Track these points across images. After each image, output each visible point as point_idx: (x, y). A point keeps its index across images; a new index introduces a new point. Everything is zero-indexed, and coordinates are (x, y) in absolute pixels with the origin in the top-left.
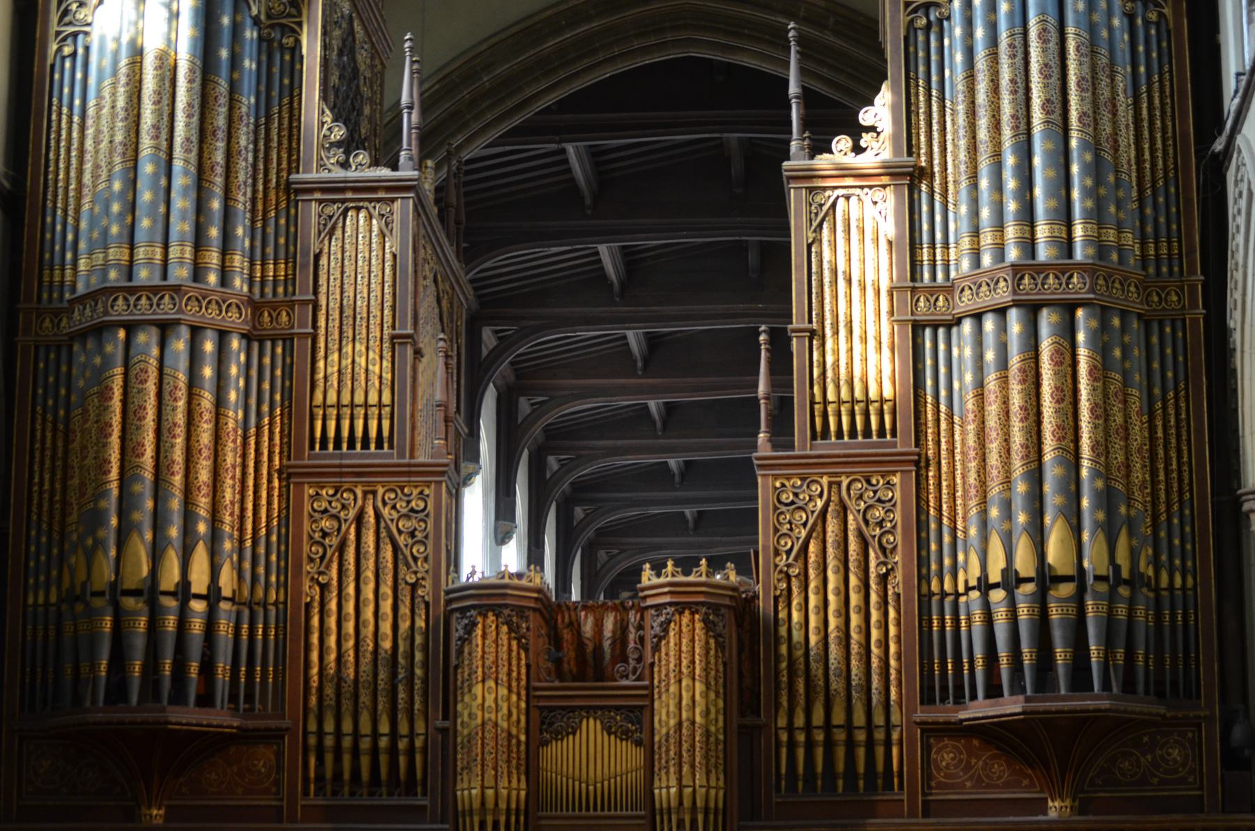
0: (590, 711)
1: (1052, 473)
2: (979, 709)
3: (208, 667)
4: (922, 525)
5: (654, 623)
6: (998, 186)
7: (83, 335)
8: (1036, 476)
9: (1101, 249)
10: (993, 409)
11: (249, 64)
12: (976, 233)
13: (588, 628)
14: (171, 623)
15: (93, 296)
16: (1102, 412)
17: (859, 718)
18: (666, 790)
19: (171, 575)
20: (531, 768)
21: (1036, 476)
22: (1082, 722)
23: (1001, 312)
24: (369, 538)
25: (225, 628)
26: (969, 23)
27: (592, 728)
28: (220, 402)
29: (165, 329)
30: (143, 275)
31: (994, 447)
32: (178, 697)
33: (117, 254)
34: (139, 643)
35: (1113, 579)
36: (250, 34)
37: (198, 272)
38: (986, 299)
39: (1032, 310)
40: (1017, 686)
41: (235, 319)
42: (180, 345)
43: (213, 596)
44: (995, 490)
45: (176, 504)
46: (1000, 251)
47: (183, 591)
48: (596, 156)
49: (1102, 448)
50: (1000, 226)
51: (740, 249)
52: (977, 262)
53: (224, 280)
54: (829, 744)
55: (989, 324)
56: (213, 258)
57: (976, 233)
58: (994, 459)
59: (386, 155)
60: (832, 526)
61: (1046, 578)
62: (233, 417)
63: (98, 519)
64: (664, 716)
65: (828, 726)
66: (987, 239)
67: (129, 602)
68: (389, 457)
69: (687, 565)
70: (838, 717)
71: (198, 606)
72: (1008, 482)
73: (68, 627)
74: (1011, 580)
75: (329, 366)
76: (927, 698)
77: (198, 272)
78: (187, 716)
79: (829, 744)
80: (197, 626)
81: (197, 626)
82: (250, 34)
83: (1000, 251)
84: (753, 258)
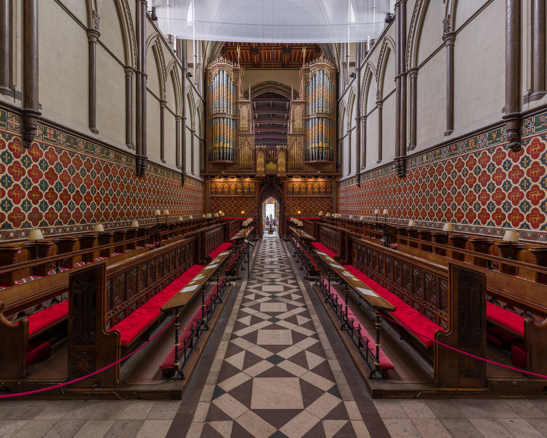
0: (271, 161)
1: (320, 136)
2: (311, 161)
3: (229, 156)
4: (305, 142)
5: (278, 152)
6: (315, 104)
7: (214, 119)
8: (318, 136)
9: (326, 112)
10: (313, 129)
11: (232, 87)
12: (312, 109)
13: (270, 152)
14: (225, 151)
15: (215, 114)
16: (325, 129)
17: (298, 162)
18: (279, 169)
19: (225, 146)
20: (265, 167)
21: (318, 136)
22: (322, 163)
23: (315, 118)
24: (246, 142)
25: (231, 152)
26: (312, 85)
27: (271, 163)
28: (230, 127)
29: (223, 118)
30: (221, 112)
31: (313, 133)
32: (226, 159)
33: (218, 109)
34: (222, 153)
35: (326, 148)
36: (232, 84)
37: (227, 112)
38: (313, 117)
39: (319, 118)
40: (315, 159)
41: (231, 117)
42: (226, 120)
43: (230, 148)
44: (313, 138)
45: (226, 138)
46: (315, 112)
47: (227, 148)
48: (257, 104)
49: (325, 133)
50: (315, 108)
51: (270, 115)
52: (312, 113)
53: (230, 113)
54: (295, 165)
55: (313, 120)
56: (229, 110)
57: (312, 109)
58: (313, 135)
59: (247, 98)
60: (296, 142)
61: (319, 148)
62: (231, 128)
63: (217, 139)
64: (279, 161)
65: (295, 163)
66: (313, 110)
67: (221, 149)
68: (247, 133)
69: (282, 145)
70: (296, 162)
71: (228, 149)
72: (315, 137)
73: (213, 152)
74: (315, 148)
75: (241, 123)
76: (305, 160)
77: (227, 112)
78: (227, 161)
79: (295, 165)
80: (228, 152)
81: (228, 152)
82: (232, 84)
83: (315, 112)
84: (271, 116)
